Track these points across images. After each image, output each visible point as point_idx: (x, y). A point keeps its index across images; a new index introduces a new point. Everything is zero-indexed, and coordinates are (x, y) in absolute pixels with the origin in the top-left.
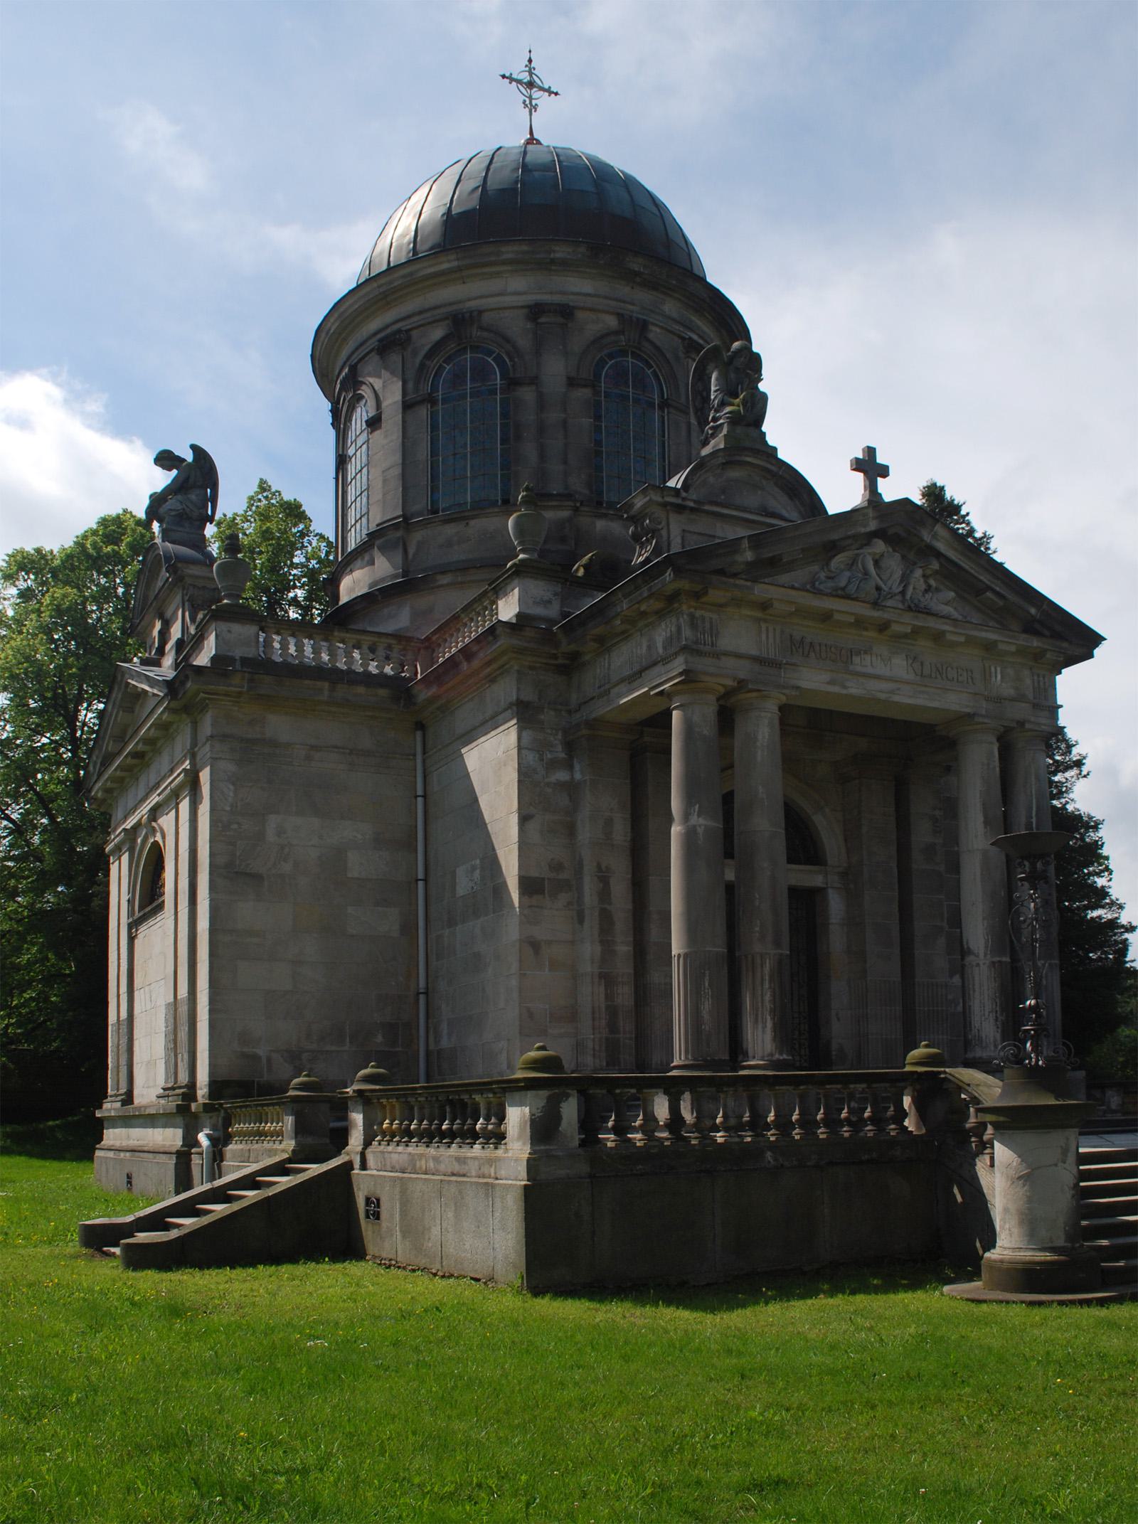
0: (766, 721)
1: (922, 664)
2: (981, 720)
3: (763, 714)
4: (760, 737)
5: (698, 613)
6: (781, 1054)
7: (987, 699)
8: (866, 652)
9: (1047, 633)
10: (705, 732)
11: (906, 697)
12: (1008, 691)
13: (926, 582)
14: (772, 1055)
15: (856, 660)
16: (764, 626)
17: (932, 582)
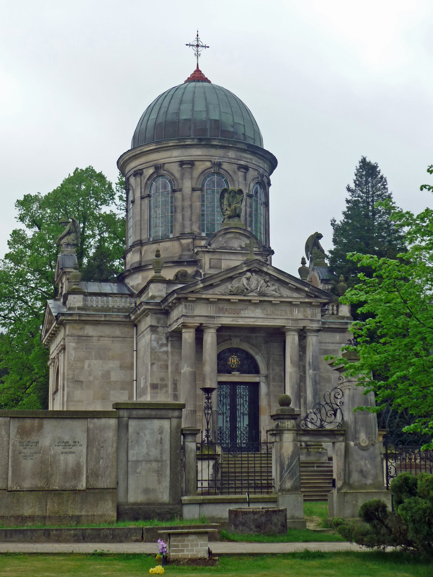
0: (210, 335)
5: (187, 304)
7: (292, 320)
8: (245, 309)
9: (313, 296)
10: (189, 341)
12: (301, 316)
16: (209, 305)
17: (269, 284)
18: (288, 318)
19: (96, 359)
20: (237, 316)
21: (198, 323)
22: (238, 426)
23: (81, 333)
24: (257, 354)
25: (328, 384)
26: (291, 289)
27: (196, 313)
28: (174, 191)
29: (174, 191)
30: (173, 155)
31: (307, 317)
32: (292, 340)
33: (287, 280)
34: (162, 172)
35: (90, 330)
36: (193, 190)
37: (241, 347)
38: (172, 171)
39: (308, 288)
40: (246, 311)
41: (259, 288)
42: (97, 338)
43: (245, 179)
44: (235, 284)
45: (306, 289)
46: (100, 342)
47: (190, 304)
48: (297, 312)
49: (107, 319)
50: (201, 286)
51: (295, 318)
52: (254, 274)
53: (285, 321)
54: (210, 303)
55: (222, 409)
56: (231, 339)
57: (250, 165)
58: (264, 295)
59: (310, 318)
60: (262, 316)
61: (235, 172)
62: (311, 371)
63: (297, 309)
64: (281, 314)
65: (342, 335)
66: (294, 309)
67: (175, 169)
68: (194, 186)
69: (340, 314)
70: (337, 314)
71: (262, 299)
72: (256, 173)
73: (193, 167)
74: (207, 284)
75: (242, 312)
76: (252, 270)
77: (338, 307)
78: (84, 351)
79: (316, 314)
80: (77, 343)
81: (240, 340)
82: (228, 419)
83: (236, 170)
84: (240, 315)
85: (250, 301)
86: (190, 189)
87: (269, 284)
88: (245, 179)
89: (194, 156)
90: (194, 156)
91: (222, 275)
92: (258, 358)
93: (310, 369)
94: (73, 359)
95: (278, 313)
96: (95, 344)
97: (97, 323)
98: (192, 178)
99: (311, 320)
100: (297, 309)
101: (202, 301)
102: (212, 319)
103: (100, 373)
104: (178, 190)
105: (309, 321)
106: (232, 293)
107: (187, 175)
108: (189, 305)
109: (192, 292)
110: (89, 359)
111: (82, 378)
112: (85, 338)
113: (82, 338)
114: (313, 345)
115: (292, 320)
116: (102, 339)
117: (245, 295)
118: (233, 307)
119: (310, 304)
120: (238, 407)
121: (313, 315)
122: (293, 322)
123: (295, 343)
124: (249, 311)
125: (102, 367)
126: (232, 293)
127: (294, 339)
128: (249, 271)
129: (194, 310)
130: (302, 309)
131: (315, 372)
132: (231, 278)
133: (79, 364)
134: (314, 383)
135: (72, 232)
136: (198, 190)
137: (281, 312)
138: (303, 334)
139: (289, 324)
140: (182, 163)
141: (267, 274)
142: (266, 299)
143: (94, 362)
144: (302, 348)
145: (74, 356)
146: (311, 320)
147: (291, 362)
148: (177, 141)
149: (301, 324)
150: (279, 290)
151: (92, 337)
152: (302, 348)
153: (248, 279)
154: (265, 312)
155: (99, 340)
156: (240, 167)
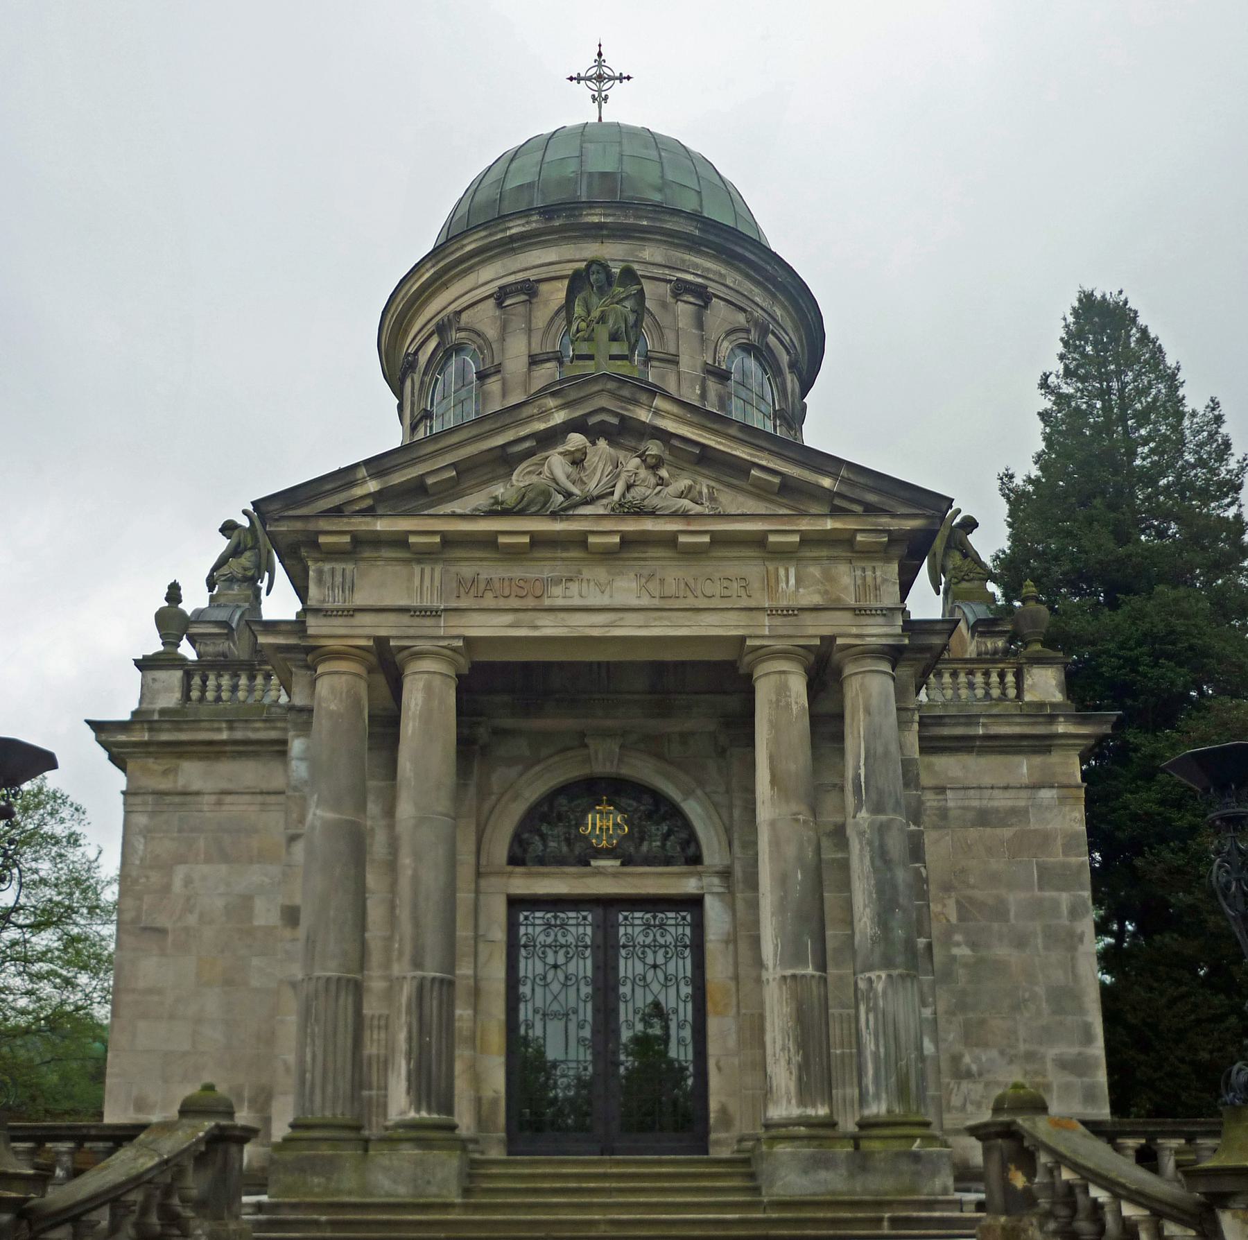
0: (421, 685)
1: (662, 581)
2: (757, 642)
4: (412, 705)
5: (327, 567)
6: (418, 1110)
7: (772, 612)
8: (570, 580)
10: (333, 707)
11: (630, 628)
13: (655, 475)
14: (403, 1113)
16: (417, 569)
17: (664, 473)
18: (753, 604)
20: (530, 602)
21: (368, 637)
23: (165, 784)
26: (761, 491)
28: (482, 376)
29: (482, 376)
30: (481, 281)
31: (839, 599)
32: (781, 695)
34: (455, 336)
35: (192, 774)
36: (534, 361)
38: (478, 327)
40: (574, 587)
42: (213, 798)
43: (700, 325)
44: (521, 478)
46: (225, 808)
47: (339, 567)
48: (792, 581)
49: (239, 735)
51: (784, 603)
52: (602, 443)
53: (742, 619)
54: (419, 561)
56: (586, 746)
58: (639, 511)
59: (851, 602)
60: (645, 601)
61: (664, 305)
62: (864, 814)
63: (792, 571)
64: (727, 593)
65: (1037, 760)
66: (782, 572)
67: (485, 318)
68: (536, 349)
69: (1028, 697)
70: (1019, 696)
71: (631, 526)
72: (741, 318)
73: (534, 300)
75: (557, 591)
77: (1019, 676)
79: (876, 588)
80: (153, 814)
81: (622, 747)
83: (670, 299)
84: (547, 602)
85: (579, 541)
86: (525, 360)
87: (664, 473)
88: (700, 325)
89: (534, 267)
90: (534, 267)
91: (460, 445)
92: (693, 809)
93: (858, 808)
94: (137, 862)
95: (709, 588)
96: (208, 814)
97: (211, 751)
98: (529, 331)
99: (858, 612)
100: (792, 571)
101: (386, 553)
102: (429, 622)
104: (493, 370)
105: (847, 617)
106: (498, 510)
107: (518, 323)
108: (333, 571)
110: (186, 863)
111: (162, 921)
112: (177, 799)
113: (168, 799)
114: (868, 711)
115: (772, 612)
117: (554, 515)
118: (517, 572)
119: (843, 543)
121: (863, 588)
122: (778, 621)
123: (788, 705)
124: (585, 584)
126: (498, 510)
127: (783, 689)
129: (352, 589)
130: (815, 571)
131: (883, 818)
132: (504, 461)
133: (155, 878)
134: (878, 863)
135: (246, 549)
136: (548, 360)
137: (726, 583)
138: (824, 671)
139: (762, 629)
142: (649, 525)
144: (826, 725)
145: (140, 853)
146: (858, 612)
147: (774, 781)
148: (483, 234)
149: (815, 628)
150: (712, 498)
151: (198, 793)
152: (826, 725)
153: (577, 460)
154: (653, 586)
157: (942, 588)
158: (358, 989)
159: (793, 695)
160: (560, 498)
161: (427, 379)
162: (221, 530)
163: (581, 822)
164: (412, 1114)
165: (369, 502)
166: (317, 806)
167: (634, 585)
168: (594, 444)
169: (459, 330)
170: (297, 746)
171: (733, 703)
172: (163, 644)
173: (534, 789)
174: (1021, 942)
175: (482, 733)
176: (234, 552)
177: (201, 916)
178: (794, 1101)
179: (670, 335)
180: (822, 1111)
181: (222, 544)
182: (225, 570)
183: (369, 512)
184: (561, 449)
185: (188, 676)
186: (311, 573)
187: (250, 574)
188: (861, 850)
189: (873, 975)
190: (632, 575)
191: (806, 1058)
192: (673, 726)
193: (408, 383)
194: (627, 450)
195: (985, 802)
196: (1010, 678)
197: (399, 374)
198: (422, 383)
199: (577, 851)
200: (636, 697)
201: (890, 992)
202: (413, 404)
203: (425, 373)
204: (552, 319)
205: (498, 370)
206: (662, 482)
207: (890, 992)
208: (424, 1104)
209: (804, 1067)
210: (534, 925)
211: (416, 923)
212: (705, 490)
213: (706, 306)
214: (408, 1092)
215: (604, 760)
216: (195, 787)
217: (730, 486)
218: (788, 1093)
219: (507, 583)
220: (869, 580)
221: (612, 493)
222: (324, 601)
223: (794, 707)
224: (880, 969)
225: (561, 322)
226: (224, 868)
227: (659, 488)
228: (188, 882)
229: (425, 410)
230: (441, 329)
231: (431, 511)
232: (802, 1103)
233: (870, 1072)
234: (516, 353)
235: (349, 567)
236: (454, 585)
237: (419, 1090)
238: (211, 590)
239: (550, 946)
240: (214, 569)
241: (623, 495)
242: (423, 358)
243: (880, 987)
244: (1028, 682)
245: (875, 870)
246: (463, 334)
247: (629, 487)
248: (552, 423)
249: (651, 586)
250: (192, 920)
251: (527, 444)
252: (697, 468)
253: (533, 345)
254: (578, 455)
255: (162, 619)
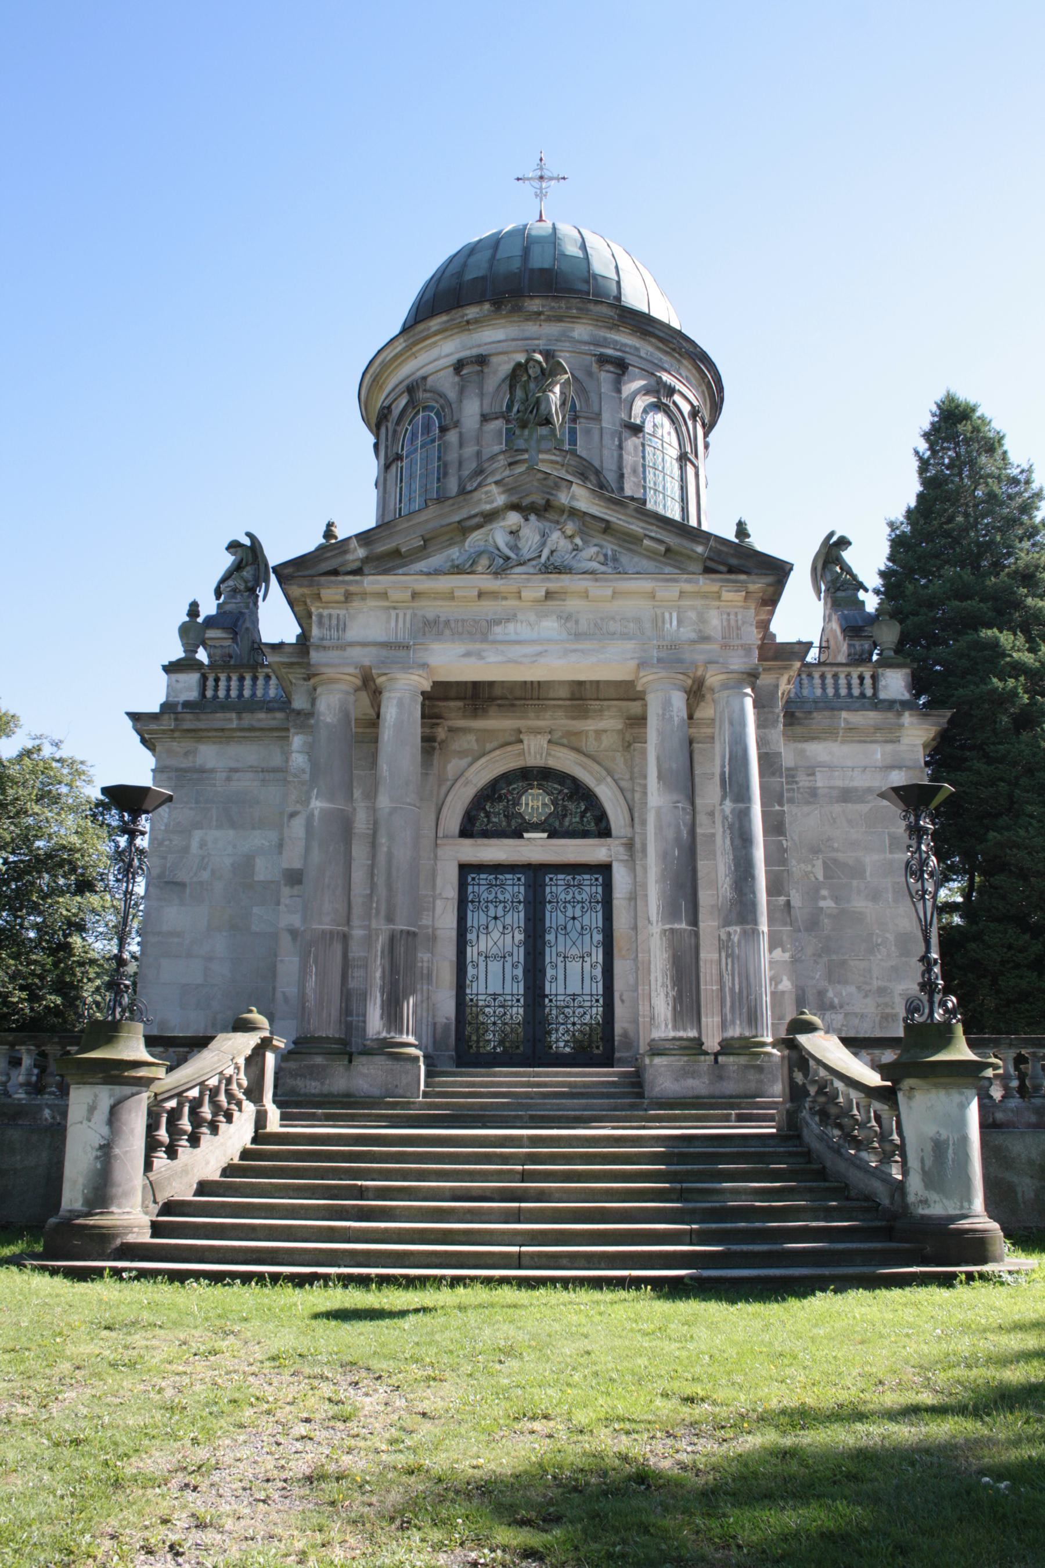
0: (395, 702)
1: (577, 622)
3: (392, 695)
4: (388, 718)
5: (326, 612)
6: (389, 1032)
8: (508, 620)
10: (328, 720)
13: (572, 542)
14: (379, 1033)
15: (498, 629)
16: (393, 613)
19: (219, 827)
22: (547, 992)
24: (600, 781)
25: (855, 883)
27: (353, 633)
29: (443, 430)
33: (636, 527)
36: (485, 418)
37: (552, 763)
39: (706, 545)
40: (511, 627)
41: (546, 553)
45: (700, 549)
48: (675, 623)
50: (361, 553)
52: (533, 518)
55: (500, 943)
56: (521, 741)
57: (630, 359)
66: (667, 615)
68: (487, 410)
74: (381, 548)
76: (525, 502)
78: (191, 808)
79: (738, 628)
81: (549, 742)
82: (519, 972)
86: (478, 418)
98: (481, 395)
103: (228, 861)
109: (335, 572)
110: (202, 828)
112: (195, 776)
114: (731, 723)
116: (236, 776)
120: (550, 937)
123: (671, 717)
124: (519, 624)
125: (235, 847)
127: (667, 704)
128: (515, 507)
129: (344, 630)
134: (737, 842)
135: (247, 565)
136: (497, 418)
140: (459, 366)
141: (574, 513)
143: (217, 833)
147: (660, 777)
155: (229, 779)
156: (603, 360)
157: (822, 595)
158: (345, 938)
159: (675, 710)
160: (501, 561)
161: (399, 429)
162: (227, 549)
163: (517, 803)
164: (384, 1034)
165: (357, 564)
166: (316, 798)
167: (556, 625)
168: (527, 520)
169: (425, 391)
170: (297, 741)
171: (635, 707)
172: (185, 651)
173: (483, 773)
174: (875, 896)
175: (441, 733)
176: (237, 568)
177: (213, 872)
178: (670, 1026)
179: (594, 397)
180: (692, 1034)
181: (228, 560)
182: (230, 583)
183: (358, 572)
184: (502, 524)
185: (204, 678)
186: (314, 617)
187: (250, 585)
188: (724, 832)
189: (731, 929)
190: (554, 617)
191: (680, 993)
192: (590, 725)
193: (383, 430)
194: (551, 522)
195: (847, 782)
196: (868, 681)
197: (374, 421)
198: (395, 431)
199: (514, 824)
200: (560, 702)
201: (743, 942)
202: (387, 447)
203: (398, 423)
204: (500, 385)
205: (457, 424)
206: (576, 548)
207: (743, 942)
208: (393, 1028)
209: (678, 999)
210: (479, 885)
211: (390, 888)
212: (610, 553)
213: (624, 373)
214: (382, 1018)
215: (536, 751)
216: (210, 765)
217: (629, 550)
218: (666, 1020)
219: (460, 624)
220: (732, 623)
221: (540, 556)
222: (322, 639)
223: (676, 719)
224: (736, 924)
225: (506, 387)
226: (231, 832)
227: (575, 553)
228: (203, 844)
229: (397, 454)
230: (411, 390)
231: (400, 571)
232: (675, 1028)
233: (728, 1004)
234: (471, 410)
235: (342, 612)
236: (421, 625)
237: (389, 1015)
238: (218, 598)
239: (492, 902)
240: (223, 581)
241: (548, 558)
242: (396, 411)
243: (736, 938)
244: (882, 683)
245: (734, 848)
246: (428, 395)
247: (552, 552)
248: (495, 505)
249: (568, 625)
250: (205, 875)
251: (477, 520)
252: (604, 537)
253: (485, 406)
254: (514, 528)
255: (184, 631)
